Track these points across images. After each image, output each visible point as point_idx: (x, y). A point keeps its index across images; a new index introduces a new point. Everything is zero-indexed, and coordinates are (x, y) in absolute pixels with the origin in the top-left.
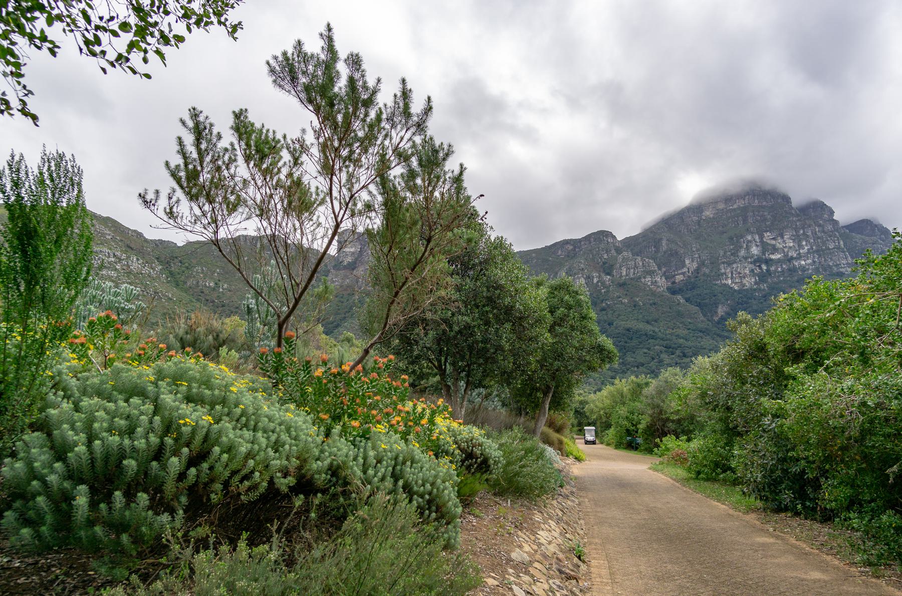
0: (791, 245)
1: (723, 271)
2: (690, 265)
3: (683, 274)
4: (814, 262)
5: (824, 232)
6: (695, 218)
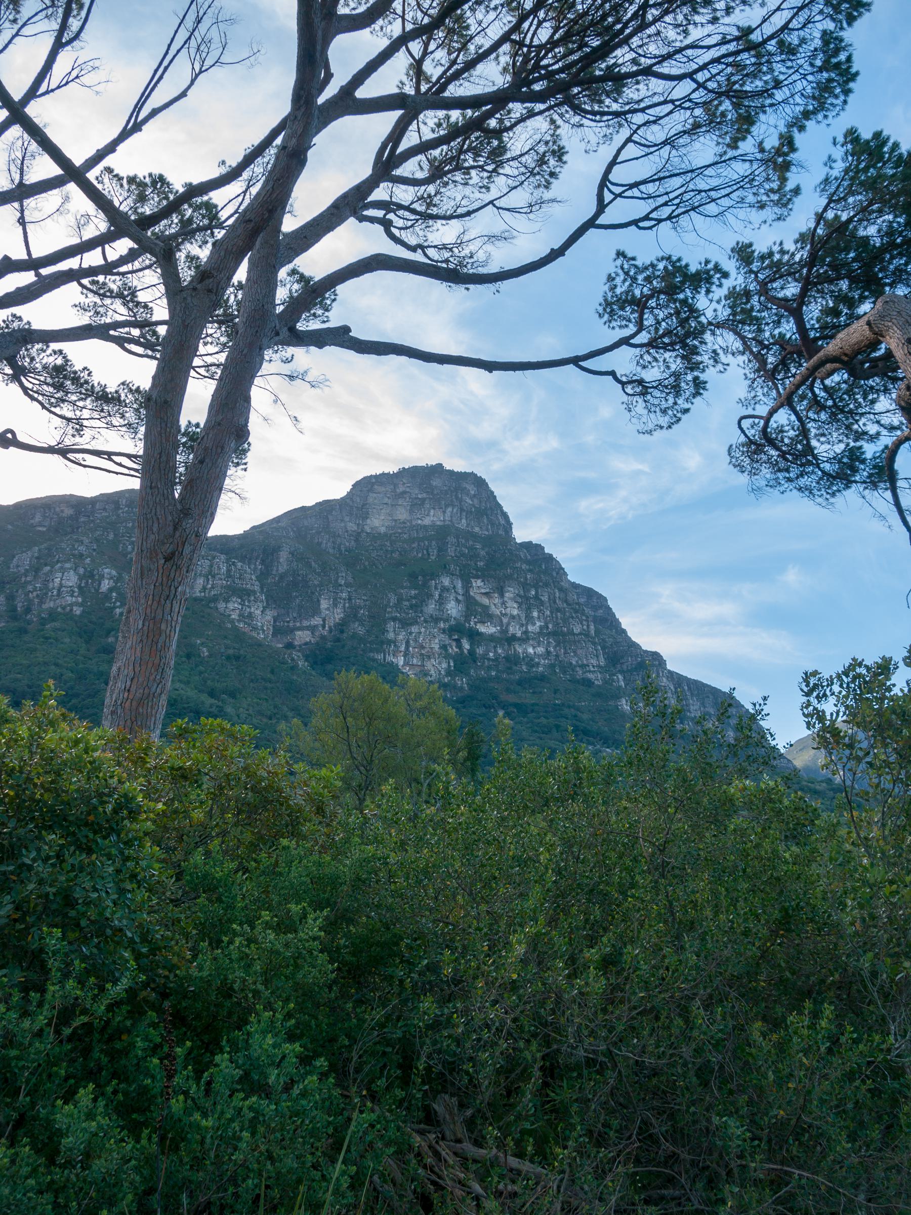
0: (515, 612)
1: (391, 636)
2: (330, 611)
3: (313, 629)
4: (548, 653)
5: (566, 601)
6: (352, 527)
